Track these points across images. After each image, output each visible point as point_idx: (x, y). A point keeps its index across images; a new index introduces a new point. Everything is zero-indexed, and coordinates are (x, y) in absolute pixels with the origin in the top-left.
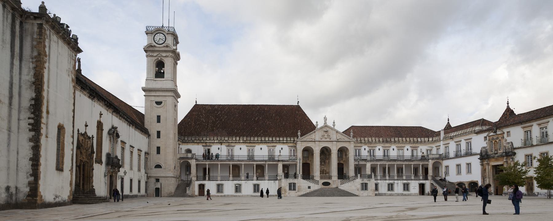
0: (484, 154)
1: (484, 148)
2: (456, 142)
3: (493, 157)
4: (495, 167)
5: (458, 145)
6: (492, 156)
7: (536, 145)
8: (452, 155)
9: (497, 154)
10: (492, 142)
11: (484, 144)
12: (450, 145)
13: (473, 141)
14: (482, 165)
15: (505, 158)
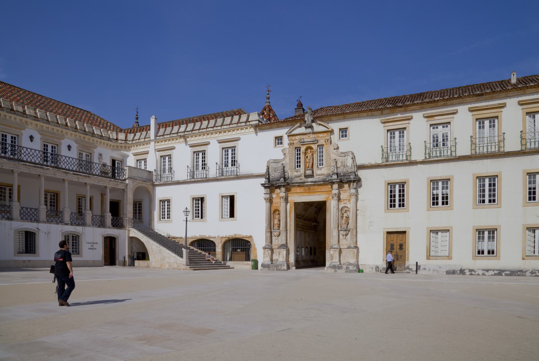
0: (274, 175)
1: (276, 161)
2: (192, 146)
3: (301, 185)
4: (296, 204)
5: (200, 154)
6: (297, 180)
7: (423, 162)
8: (181, 172)
9: (312, 176)
10: (298, 149)
11: (277, 153)
12: (174, 153)
13: (240, 147)
14: (270, 201)
15: (336, 186)
